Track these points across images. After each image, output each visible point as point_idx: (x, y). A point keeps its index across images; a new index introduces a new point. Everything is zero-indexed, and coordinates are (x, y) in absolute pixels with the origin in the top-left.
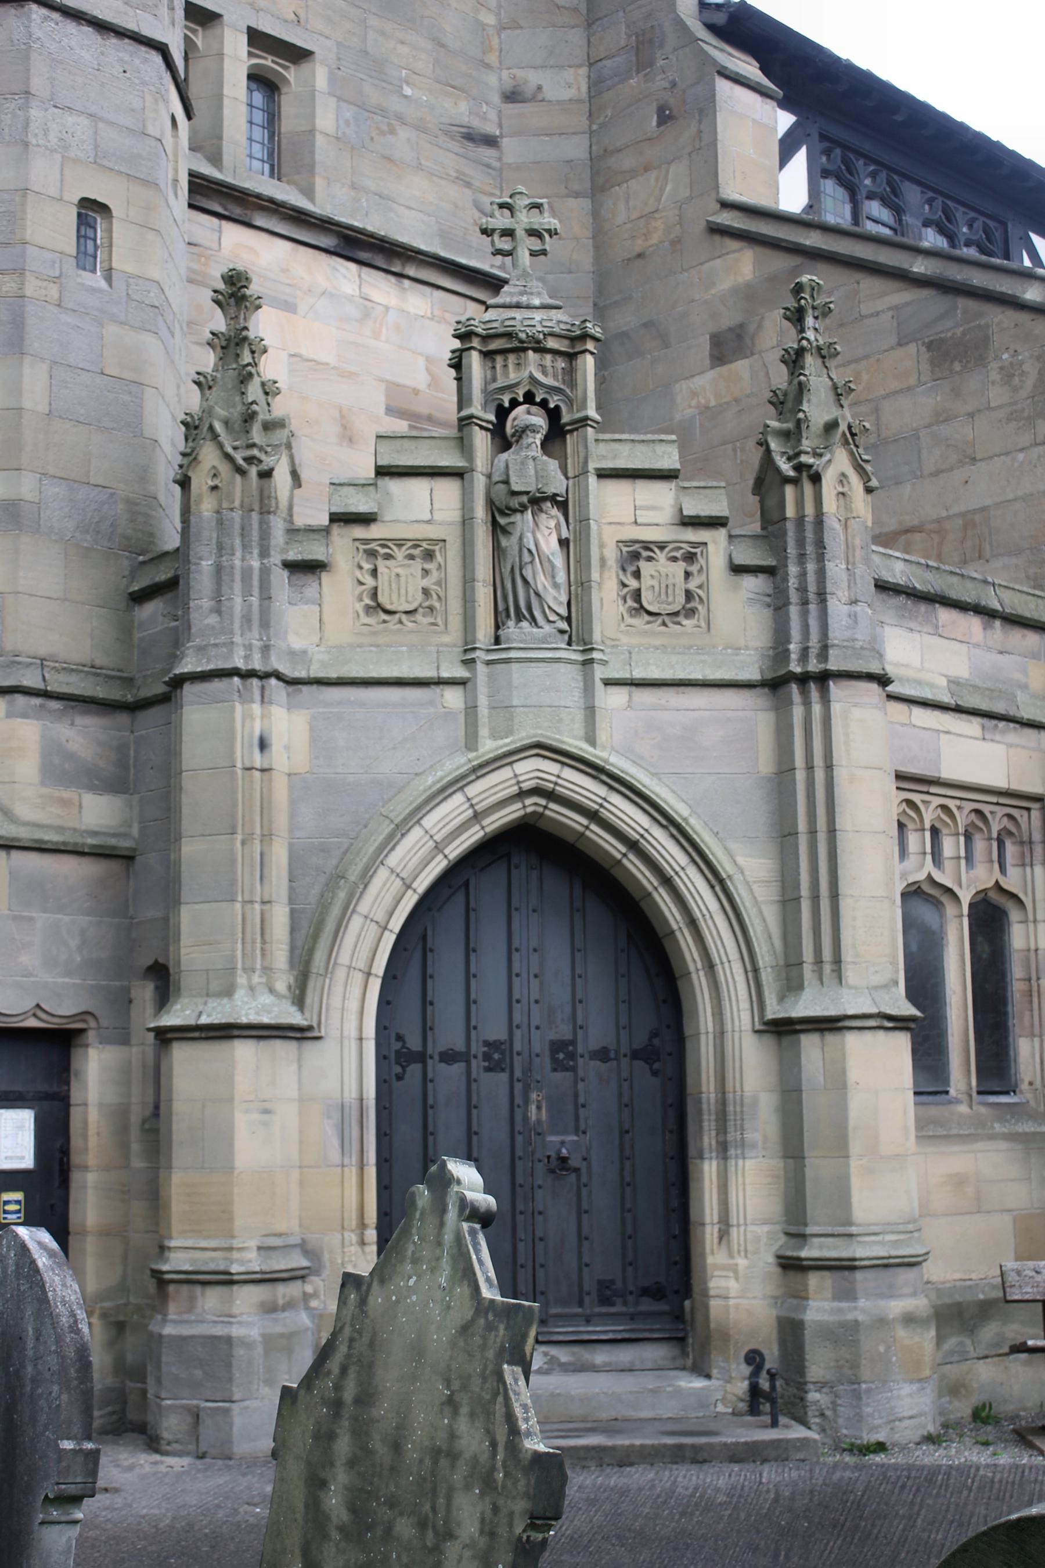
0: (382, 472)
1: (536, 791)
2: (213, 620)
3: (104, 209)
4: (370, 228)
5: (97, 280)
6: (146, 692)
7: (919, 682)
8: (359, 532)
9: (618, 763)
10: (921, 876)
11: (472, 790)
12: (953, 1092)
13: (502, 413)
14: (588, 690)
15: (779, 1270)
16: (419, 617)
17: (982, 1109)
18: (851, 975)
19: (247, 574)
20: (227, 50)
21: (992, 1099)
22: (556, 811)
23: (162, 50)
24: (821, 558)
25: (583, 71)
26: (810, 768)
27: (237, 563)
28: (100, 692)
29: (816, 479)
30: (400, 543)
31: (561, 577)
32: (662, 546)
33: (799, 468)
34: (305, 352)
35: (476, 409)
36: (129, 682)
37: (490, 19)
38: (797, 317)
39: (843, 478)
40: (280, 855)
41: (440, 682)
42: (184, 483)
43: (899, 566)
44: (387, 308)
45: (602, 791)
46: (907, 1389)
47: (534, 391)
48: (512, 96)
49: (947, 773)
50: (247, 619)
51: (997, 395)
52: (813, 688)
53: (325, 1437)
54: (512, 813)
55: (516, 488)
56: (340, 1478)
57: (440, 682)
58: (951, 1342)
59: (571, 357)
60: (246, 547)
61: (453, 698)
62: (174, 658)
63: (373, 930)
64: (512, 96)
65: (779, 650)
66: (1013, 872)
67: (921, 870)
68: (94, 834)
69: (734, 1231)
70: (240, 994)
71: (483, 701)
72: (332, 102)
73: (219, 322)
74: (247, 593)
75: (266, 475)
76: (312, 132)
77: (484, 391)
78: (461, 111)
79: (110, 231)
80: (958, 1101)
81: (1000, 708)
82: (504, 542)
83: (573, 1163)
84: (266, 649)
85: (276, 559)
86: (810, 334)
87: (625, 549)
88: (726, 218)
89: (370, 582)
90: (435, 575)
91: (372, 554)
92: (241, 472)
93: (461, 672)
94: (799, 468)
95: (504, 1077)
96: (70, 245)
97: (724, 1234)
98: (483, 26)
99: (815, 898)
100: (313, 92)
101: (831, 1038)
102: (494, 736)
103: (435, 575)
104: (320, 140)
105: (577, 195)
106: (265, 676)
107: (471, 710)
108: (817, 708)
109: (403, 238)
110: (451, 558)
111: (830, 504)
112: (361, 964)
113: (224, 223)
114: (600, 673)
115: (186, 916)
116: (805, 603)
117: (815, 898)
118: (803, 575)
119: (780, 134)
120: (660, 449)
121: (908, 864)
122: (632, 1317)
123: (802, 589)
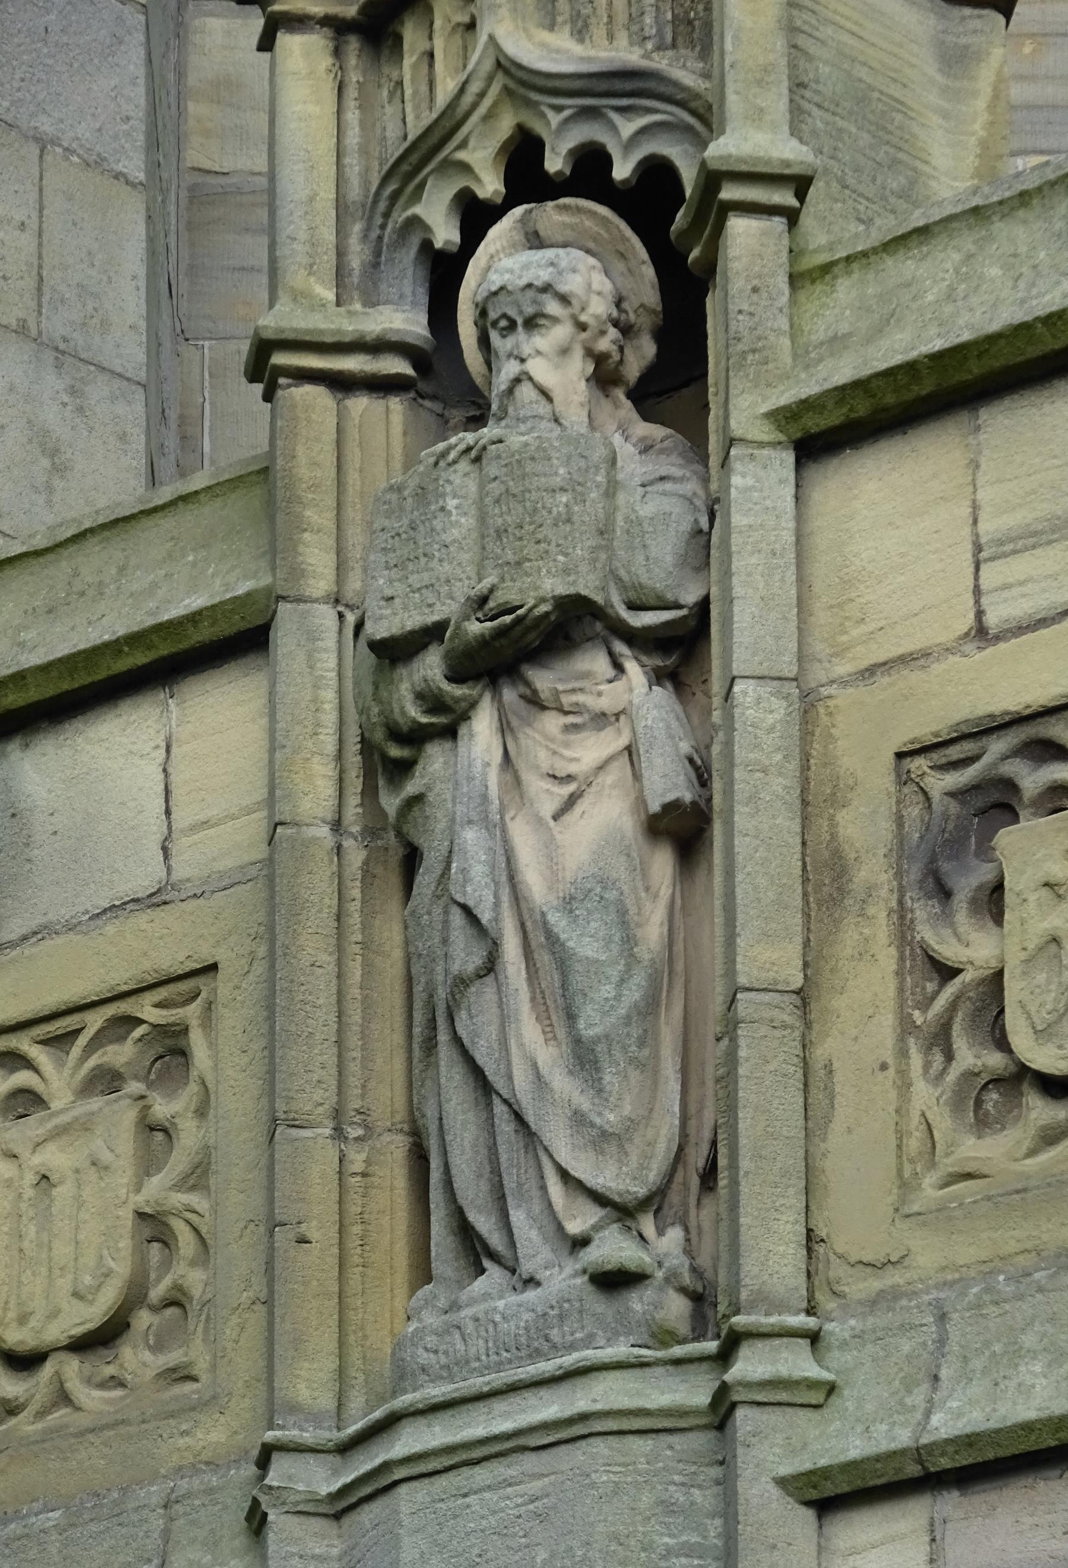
47: (538, 128)
87: (940, 784)
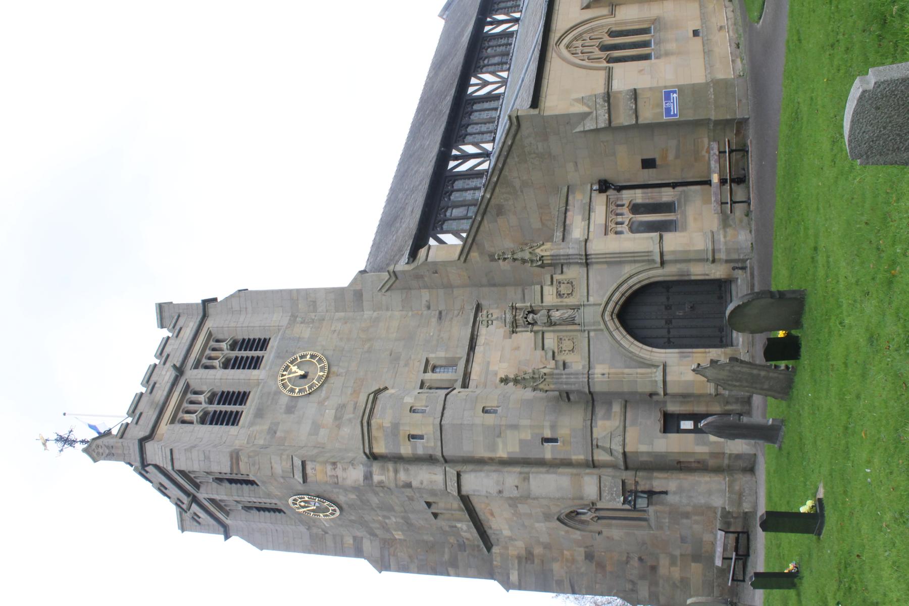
0: (543, 349)
1: (612, 316)
2: (577, 385)
3: (484, 408)
4: (468, 344)
5: (499, 410)
6: (591, 399)
7: (584, 229)
8: (556, 354)
9: (605, 299)
10: (627, 228)
11: (612, 330)
12: (675, 219)
13: (529, 323)
14: (590, 305)
15: (715, 264)
16: (574, 341)
17: (679, 211)
18: (651, 249)
19: (567, 378)
20: (429, 378)
21: (676, 208)
22: (616, 311)
23: (447, 395)
24: (560, 255)
25: (422, 290)
26: (605, 258)
27: (564, 380)
28: (590, 408)
29: (542, 256)
30: (558, 345)
31: (565, 311)
32: (557, 289)
33: (540, 260)
34: (499, 359)
35: (529, 329)
36: (587, 402)
37: (410, 313)
38: (505, 259)
39: (542, 250)
40: (627, 371)
41: (589, 337)
42: (547, 391)
43: (558, 233)
44: (486, 339)
45: (611, 302)
46: (740, 237)
48: (429, 308)
49: (604, 222)
50: (576, 378)
51: (511, 202)
52: (588, 257)
53: (729, 385)
54: (616, 321)
55: (546, 321)
56: (735, 383)
57: (589, 337)
58: (731, 223)
59: (516, 309)
60: (561, 378)
61: (592, 334)
62: (585, 394)
63: (642, 351)
64: (429, 308)
65: (581, 263)
66: (624, 202)
67: (625, 228)
68: (621, 409)
69: (707, 273)
70: (657, 379)
71: (593, 328)
72: (437, 353)
73: (511, 384)
74: (571, 378)
75: (545, 374)
76: (445, 358)
77: (525, 327)
78: (434, 320)
79: (488, 407)
80: (677, 218)
81: (588, 208)
82: (558, 323)
83: (692, 305)
84: (583, 374)
85: (563, 372)
86: (509, 256)
88: (462, 259)
89: (567, 352)
90: (565, 338)
91: (561, 351)
92: (545, 380)
93: (586, 333)
94: (540, 260)
95: (673, 321)
96: (493, 415)
97: (707, 275)
98: (412, 315)
99: (634, 257)
100: (436, 358)
101: (665, 254)
102: (600, 325)
103: (565, 338)
104: (447, 356)
105: (453, 292)
106: (589, 374)
107: (595, 330)
108: (593, 256)
109: (469, 336)
110: (561, 335)
111: (548, 253)
112: (649, 353)
113: (471, 378)
114: (586, 303)
115: (640, 390)
116: (569, 259)
117: (634, 257)
118: (564, 259)
119: (438, 244)
120: (536, 289)
121: (624, 230)
122: (726, 292)
123: (566, 259)
